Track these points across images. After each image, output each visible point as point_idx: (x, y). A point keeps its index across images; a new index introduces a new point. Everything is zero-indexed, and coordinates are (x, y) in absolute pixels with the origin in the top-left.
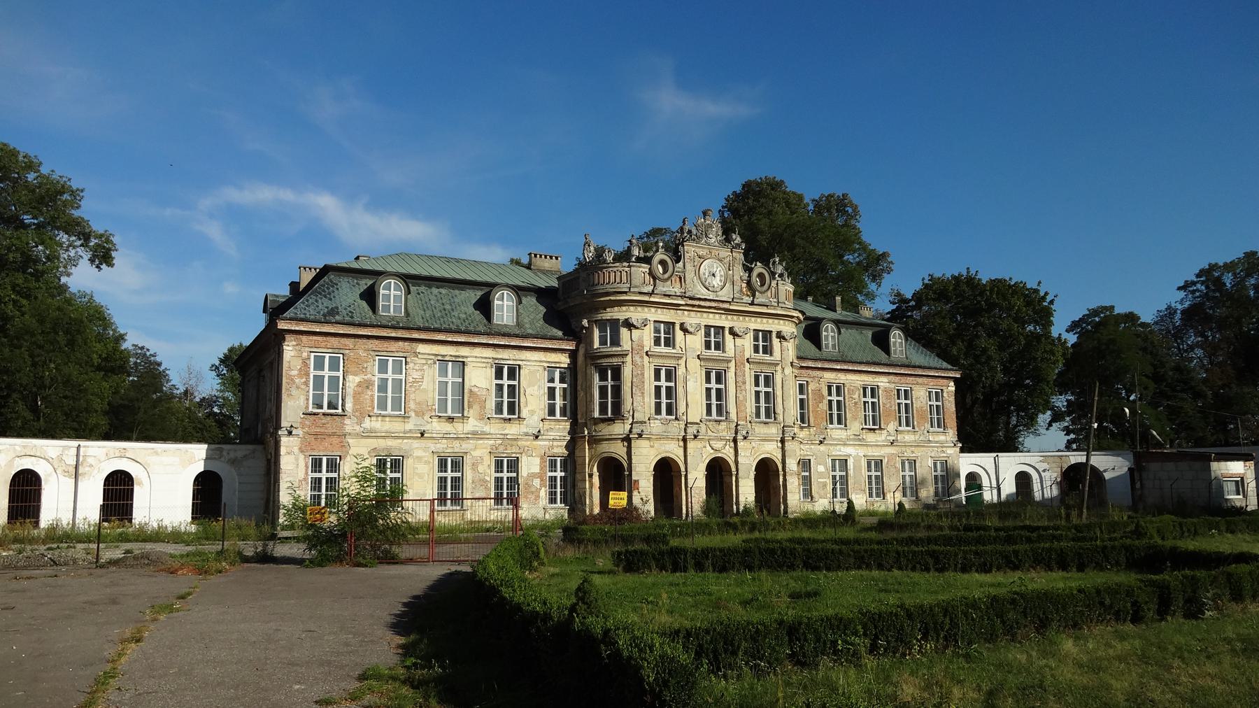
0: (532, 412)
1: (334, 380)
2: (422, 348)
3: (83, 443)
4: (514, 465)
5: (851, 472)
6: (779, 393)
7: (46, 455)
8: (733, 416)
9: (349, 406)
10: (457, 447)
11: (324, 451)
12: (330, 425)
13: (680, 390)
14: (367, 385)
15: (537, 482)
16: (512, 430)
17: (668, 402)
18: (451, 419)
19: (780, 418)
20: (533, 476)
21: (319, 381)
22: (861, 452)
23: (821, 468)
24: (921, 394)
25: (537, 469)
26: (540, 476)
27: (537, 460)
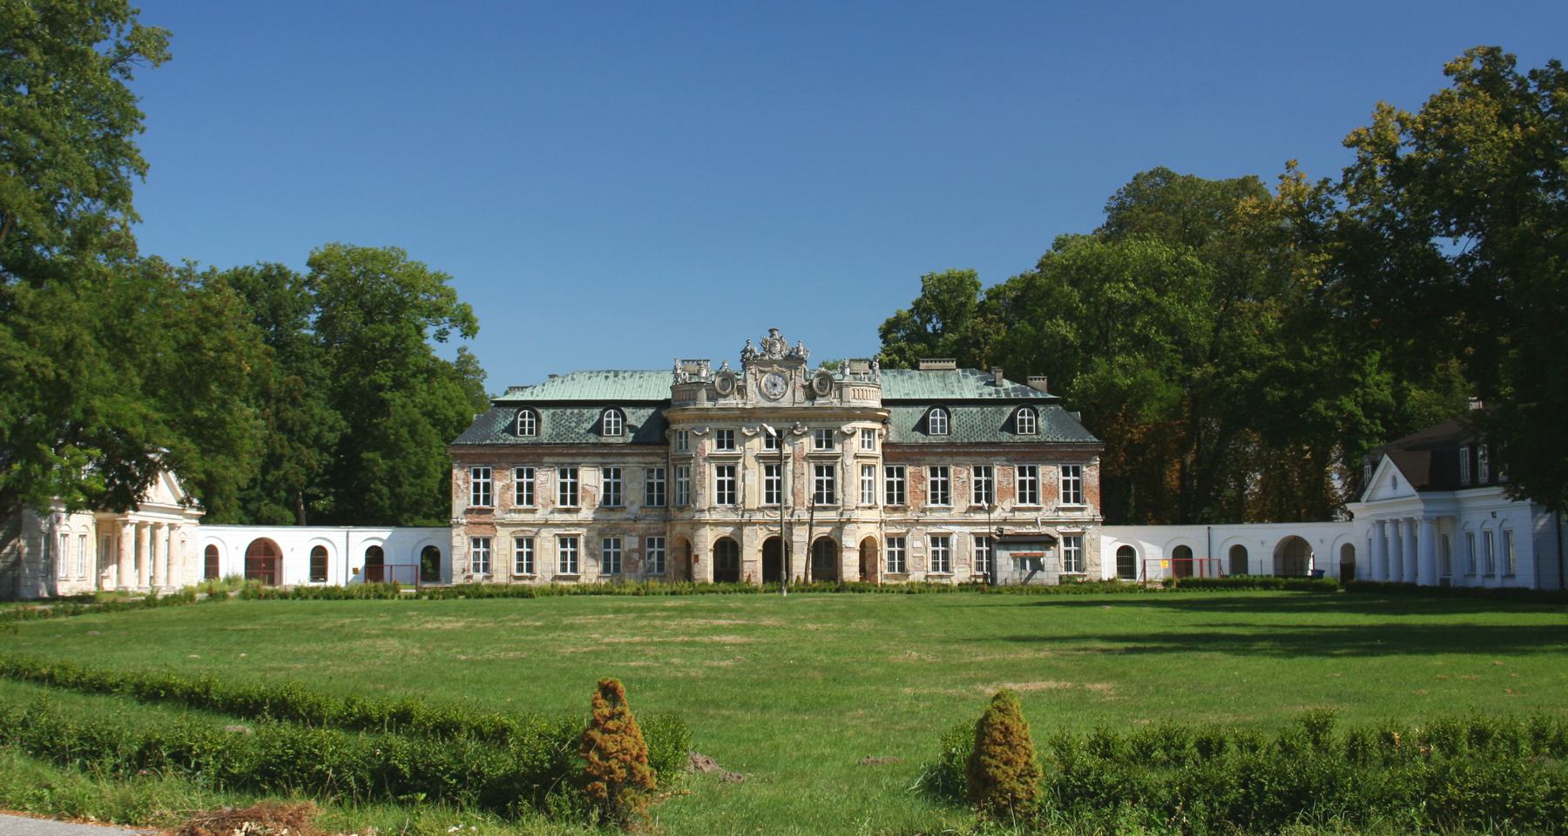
0: (632, 503)
1: (487, 486)
2: (546, 459)
3: (351, 529)
4: (617, 544)
5: (954, 548)
6: (839, 481)
7: (333, 538)
8: (790, 503)
9: (496, 503)
10: (573, 531)
11: (481, 532)
12: (484, 518)
13: (739, 483)
14: (508, 487)
15: (636, 556)
16: (616, 516)
17: (728, 493)
18: (568, 511)
19: (840, 503)
20: (633, 551)
21: (477, 486)
22: (967, 529)
23: (918, 544)
24: (1050, 474)
25: (636, 546)
26: (640, 551)
27: (636, 540)
